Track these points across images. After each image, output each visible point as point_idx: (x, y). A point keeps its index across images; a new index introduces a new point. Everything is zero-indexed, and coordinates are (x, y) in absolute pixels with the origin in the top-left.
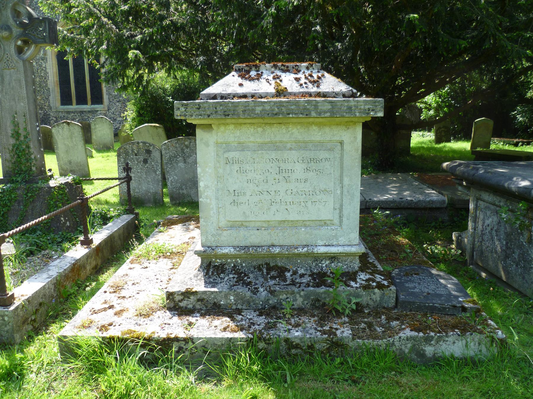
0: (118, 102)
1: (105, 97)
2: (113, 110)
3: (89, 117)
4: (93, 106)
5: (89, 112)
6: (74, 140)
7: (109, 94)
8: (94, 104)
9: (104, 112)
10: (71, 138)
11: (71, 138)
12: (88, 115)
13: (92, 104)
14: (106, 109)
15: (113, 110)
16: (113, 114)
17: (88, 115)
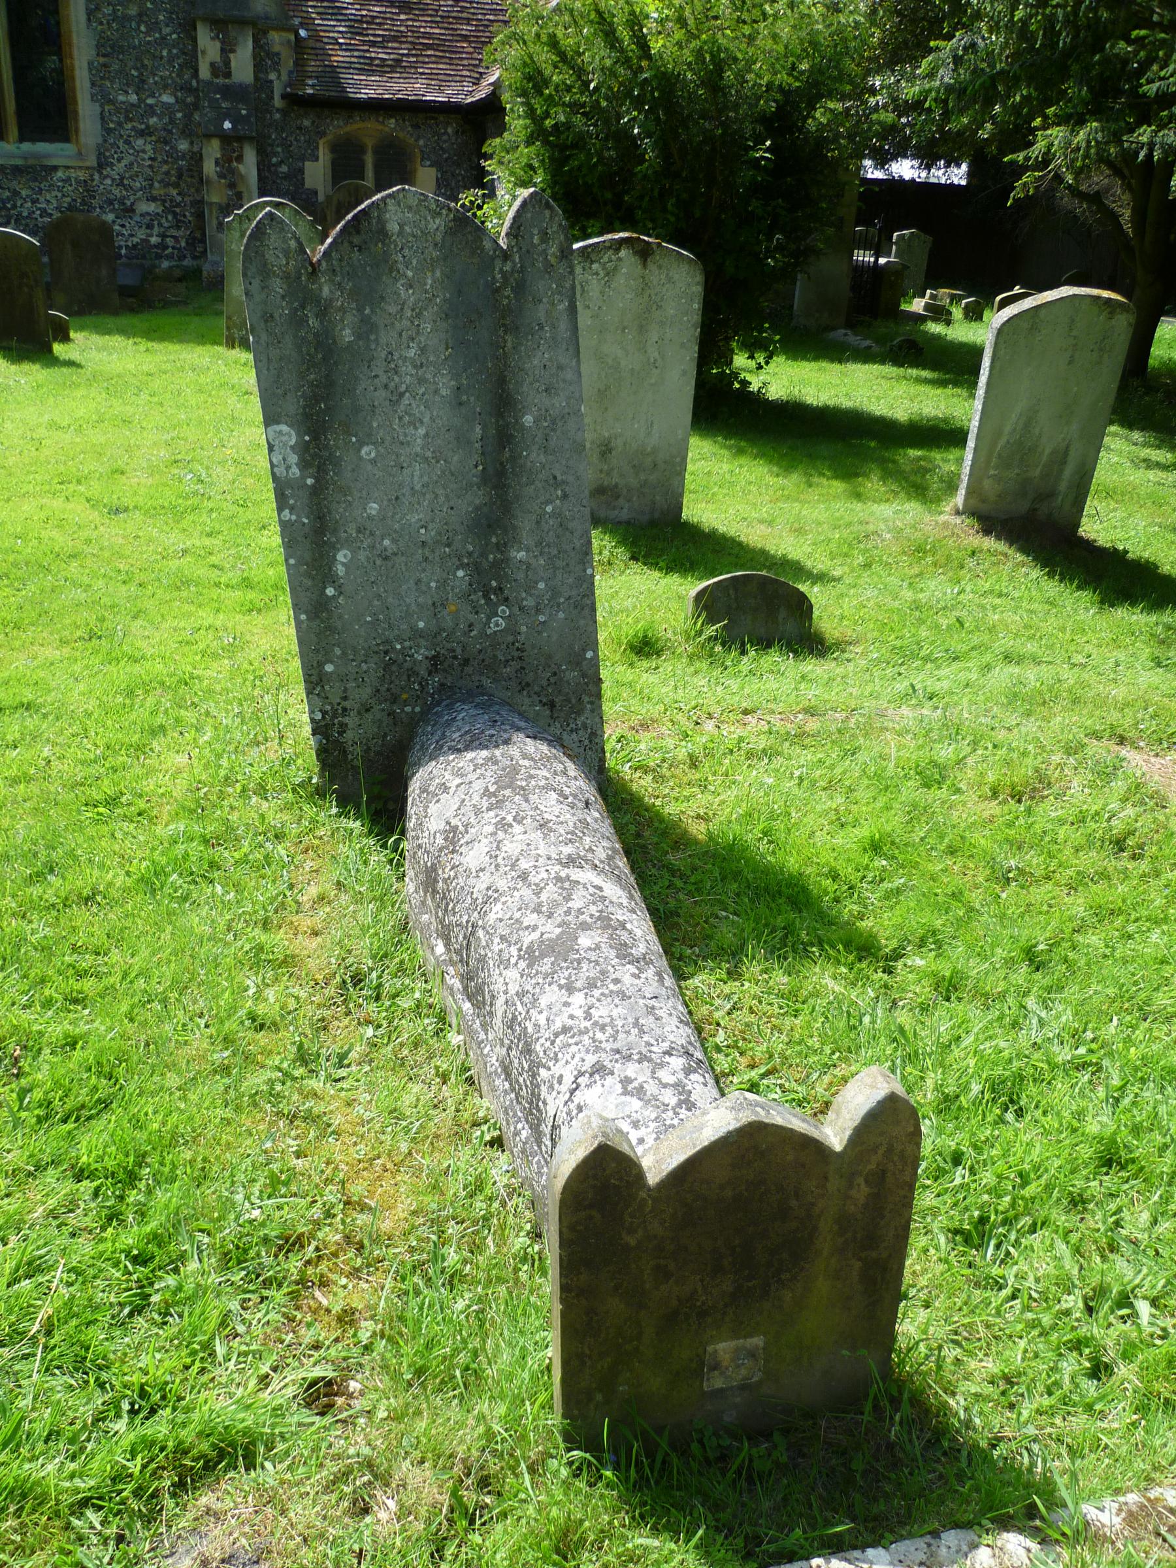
0: (142, 134)
1: (87, 111)
2: (120, 167)
3: (16, 193)
4: (26, 146)
5: (17, 170)
6: (654, 336)
7: (102, 97)
8: (33, 140)
9: (82, 175)
10: (642, 329)
11: (642, 329)
12: (14, 185)
13: (22, 139)
14: (92, 161)
15: (120, 167)
16: (121, 184)
17: (14, 185)
